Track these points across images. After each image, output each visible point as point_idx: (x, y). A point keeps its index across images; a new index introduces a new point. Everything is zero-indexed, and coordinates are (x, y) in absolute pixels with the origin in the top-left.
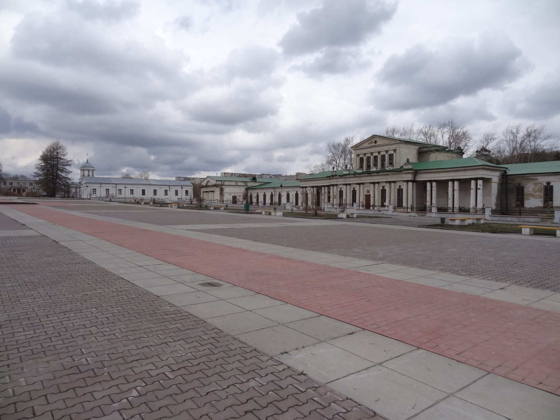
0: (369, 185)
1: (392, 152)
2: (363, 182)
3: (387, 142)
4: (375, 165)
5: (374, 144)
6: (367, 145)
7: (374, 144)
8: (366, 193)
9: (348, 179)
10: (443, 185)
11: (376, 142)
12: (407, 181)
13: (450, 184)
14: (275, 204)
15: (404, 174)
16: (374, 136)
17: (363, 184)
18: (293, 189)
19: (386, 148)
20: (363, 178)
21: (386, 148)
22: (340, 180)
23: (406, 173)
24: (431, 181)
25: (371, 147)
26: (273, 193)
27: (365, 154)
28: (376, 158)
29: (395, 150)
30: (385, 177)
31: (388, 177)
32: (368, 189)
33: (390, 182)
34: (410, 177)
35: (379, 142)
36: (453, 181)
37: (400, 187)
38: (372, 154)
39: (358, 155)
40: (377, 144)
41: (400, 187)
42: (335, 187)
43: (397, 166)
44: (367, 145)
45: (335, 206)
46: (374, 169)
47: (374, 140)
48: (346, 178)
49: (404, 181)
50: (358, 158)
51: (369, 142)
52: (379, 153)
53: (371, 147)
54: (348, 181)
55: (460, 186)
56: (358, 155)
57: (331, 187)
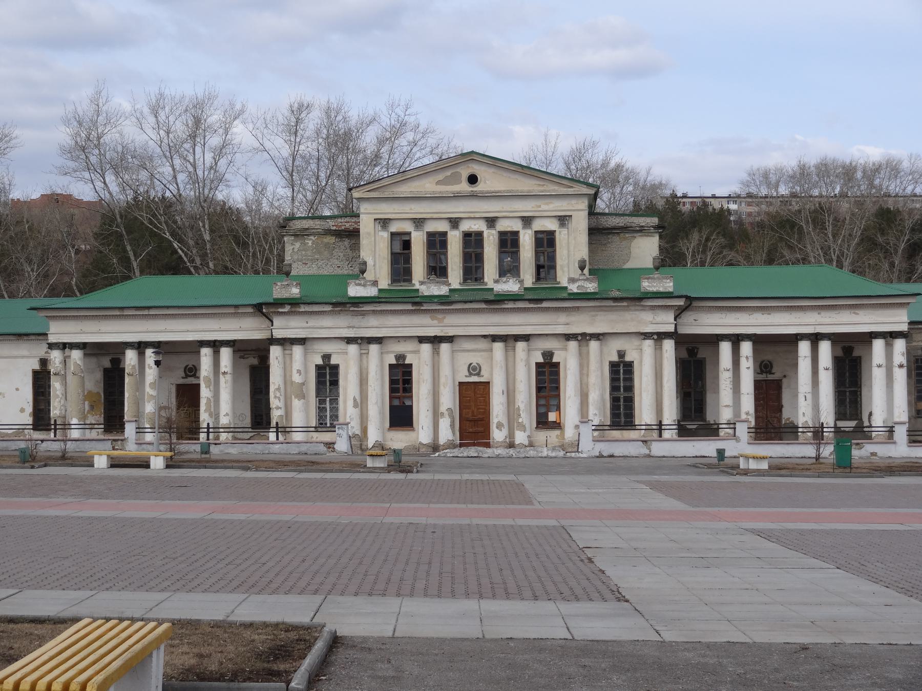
0: (483, 344)
1: (551, 225)
2: (451, 332)
4: (509, 269)
5: (464, 187)
6: (428, 186)
8: (463, 377)
9: (373, 321)
10: (774, 351)
11: (473, 179)
12: (661, 336)
13: (804, 347)
15: (644, 308)
16: (471, 157)
17: (450, 339)
20: (451, 319)
22: (327, 321)
23: (653, 308)
24: (736, 340)
25: (457, 197)
29: (563, 220)
30: (562, 318)
32: (475, 359)
33: (583, 338)
34: (665, 321)
35: (490, 181)
36: (815, 339)
37: (621, 354)
40: (480, 187)
41: (621, 354)
42: (297, 350)
44: (428, 186)
45: (223, 437)
46: (511, 286)
47: (465, 173)
48: (363, 314)
49: (646, 336)
50: (385, 235)
51: (441, 176)
52: (491, 222)
53: (457, 197)
54: (372, 326)
55: (755, 351)
56: (384, 223)
57: (275, 352)
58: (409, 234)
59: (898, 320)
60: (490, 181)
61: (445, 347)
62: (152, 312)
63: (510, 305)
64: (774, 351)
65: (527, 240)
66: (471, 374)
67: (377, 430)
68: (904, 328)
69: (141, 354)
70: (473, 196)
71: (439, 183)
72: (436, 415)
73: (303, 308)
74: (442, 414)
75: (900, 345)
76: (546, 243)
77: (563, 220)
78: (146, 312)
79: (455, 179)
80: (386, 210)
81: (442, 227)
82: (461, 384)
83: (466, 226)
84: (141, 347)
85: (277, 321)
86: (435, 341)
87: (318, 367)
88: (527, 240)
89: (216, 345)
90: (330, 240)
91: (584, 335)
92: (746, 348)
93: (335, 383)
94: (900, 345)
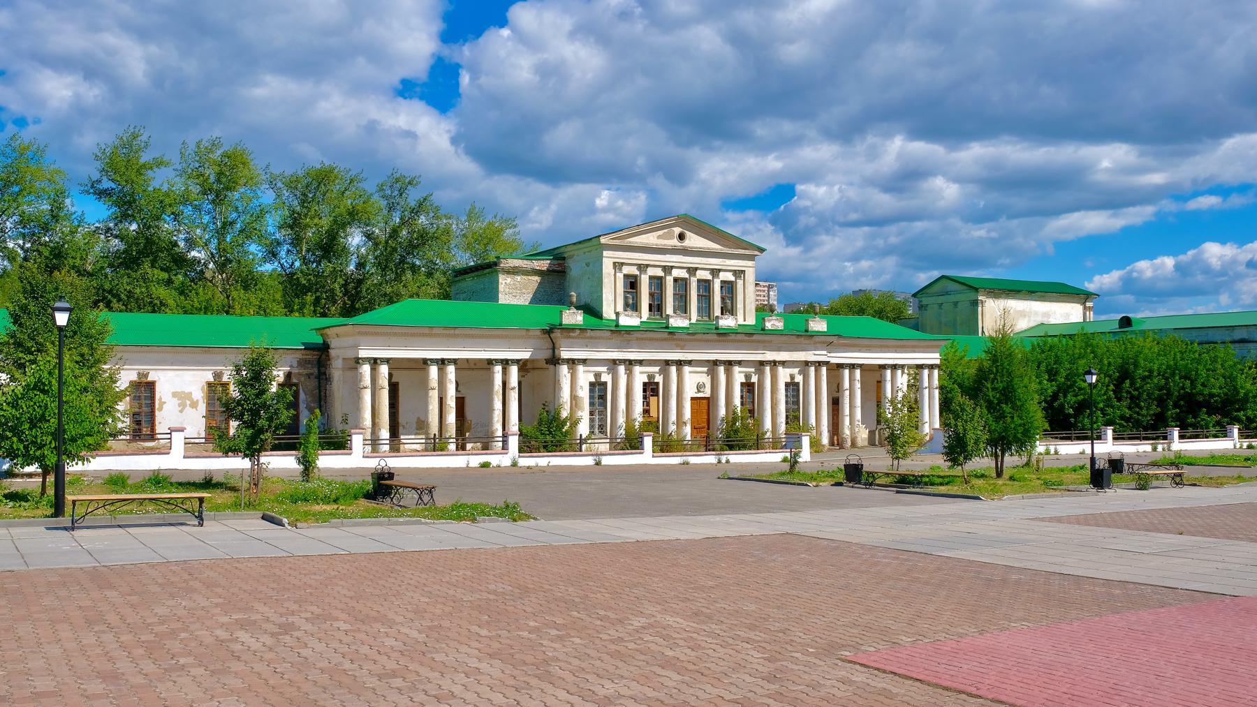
1: (730, 277)
5: (675, 242)
6: (651, 239)
7: (675, 242)
11: (681, 237)
17: (689, 363)
19: (715, 262)
28: (681, 284)
29: (739, 273)
39: (618, 266)
40: (687, 243)
43: (745, 316)
46: (727, 322)
47: (677, 230)
50: (620, 276)
51: (660, 233)
56: (618, 266)
58: (635, 277)
59: (934, 358)
61: (687, 369)
62: (457, 332)
63: (733, 337)
64: (873, 376)
66: (699, 391)
68: (938, 362)
69: (442, 373)
71: (659, 237)
73: (589, 333)
74: (685, 423)
75: (936, 372)
76: (729, 288)
78: (452, 332)
79: (670, 236)
81: (659, 273)
82: (692, 399)
83: (676, 273)
84: (442, 363)
86: (680, 363)
87: (592, 384)
89: (506, 363)
91: (775, 362)
92: (858, 372)
93: (603, 397)
94: (936, 372)
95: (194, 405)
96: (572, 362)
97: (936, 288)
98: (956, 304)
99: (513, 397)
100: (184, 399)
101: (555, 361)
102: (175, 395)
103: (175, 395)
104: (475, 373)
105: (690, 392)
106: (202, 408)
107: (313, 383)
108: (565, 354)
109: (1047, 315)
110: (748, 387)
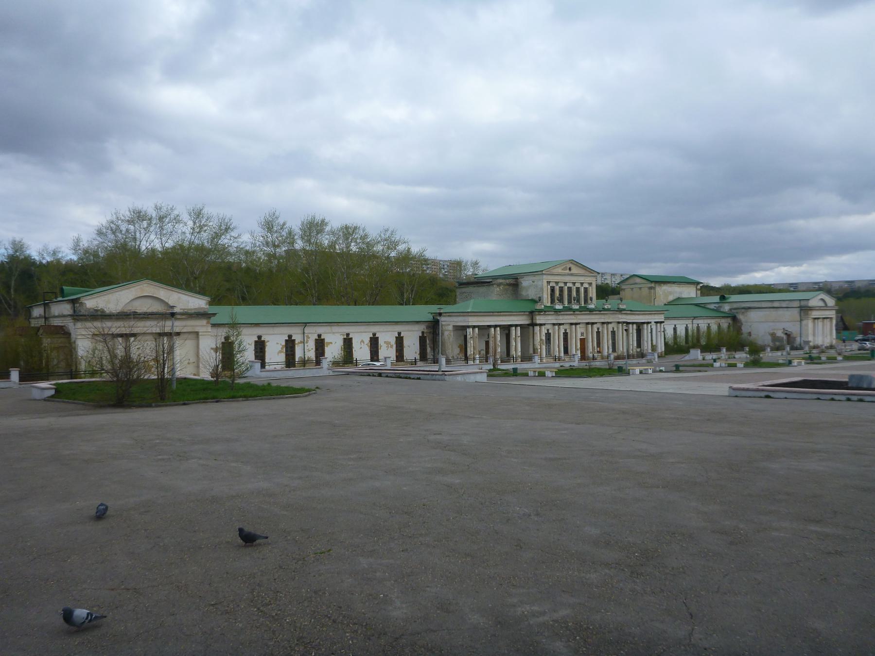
3: (582, 272)
5: (568, 271)
9: (561, 317)
11: (570, 269)
14: (304, 363)
18: (362, 328)
19: (582, 279)
21: (582, 279)
26: (298, 338)
27: (557, 283)
29: (590, 284)
30: (603, 317)
31: (606, 316)
38: (566, 283)
39: (548, 283)
44: (559, 270)
54: (562, 319)
56: (548, 283)
60: (575, 270)
65: (582, 290)
67: (562, 354)
70: (572, 275)
72: (576, 349)
77: (590, 284)
80: (550, 278)
85: (538, 317)
86: (576, 324)
88: (582, 290)
90: (507, 287)
95: (392, 347)
96: (541, 325)
97: (631, 281)
98: (640, 288)
99: (519, 340)
100: (387, 343)
101: (533, 325)
102: (385, 342)
103: (385, 342)
104: (506, 330)
105: (579, 336)
106: (395, 346)
107: (431, 336)
108: (538, 322)
109: (681, 293)
110: (598, 333)
